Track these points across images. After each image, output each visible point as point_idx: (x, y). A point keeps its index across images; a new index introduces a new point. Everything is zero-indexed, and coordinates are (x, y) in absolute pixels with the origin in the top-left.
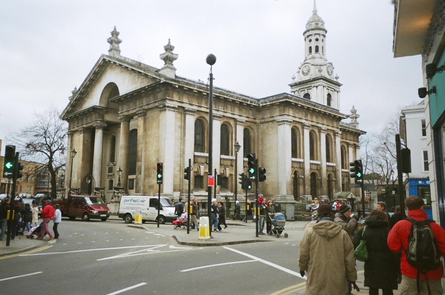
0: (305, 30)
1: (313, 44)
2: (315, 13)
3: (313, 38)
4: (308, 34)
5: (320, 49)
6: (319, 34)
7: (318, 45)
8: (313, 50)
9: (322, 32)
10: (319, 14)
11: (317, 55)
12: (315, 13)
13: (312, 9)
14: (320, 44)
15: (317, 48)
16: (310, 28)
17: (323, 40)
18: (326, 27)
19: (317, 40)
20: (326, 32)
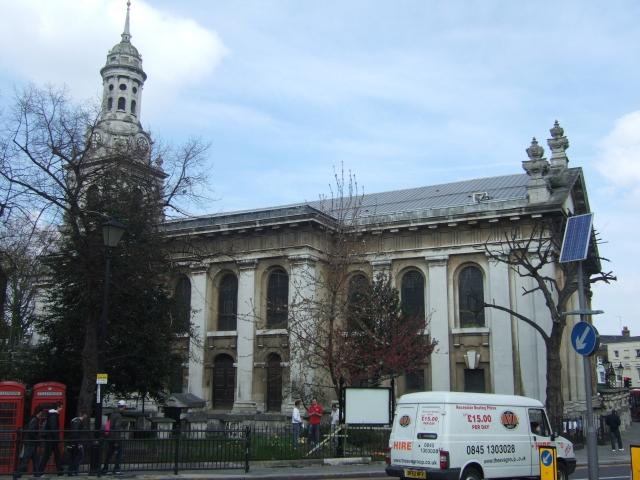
0: (103, 65)
1: (117, 94)
2: (126, 37)
3: (116, 84)
4: (110, 73)
5: (128, 105)
6: (127, 77)
7: (124, 96)
8: (115, 103)
9: (133, 75)
10: (134, 42)
11: (121, 116)
12: (126, 37)
13: (122, 31)
14: (128, 95)
15: (122, 101)
16: (115, 63)
17: (135, 90)
18: (145, 68)
19: (123, 87)
20: (145, 77)
